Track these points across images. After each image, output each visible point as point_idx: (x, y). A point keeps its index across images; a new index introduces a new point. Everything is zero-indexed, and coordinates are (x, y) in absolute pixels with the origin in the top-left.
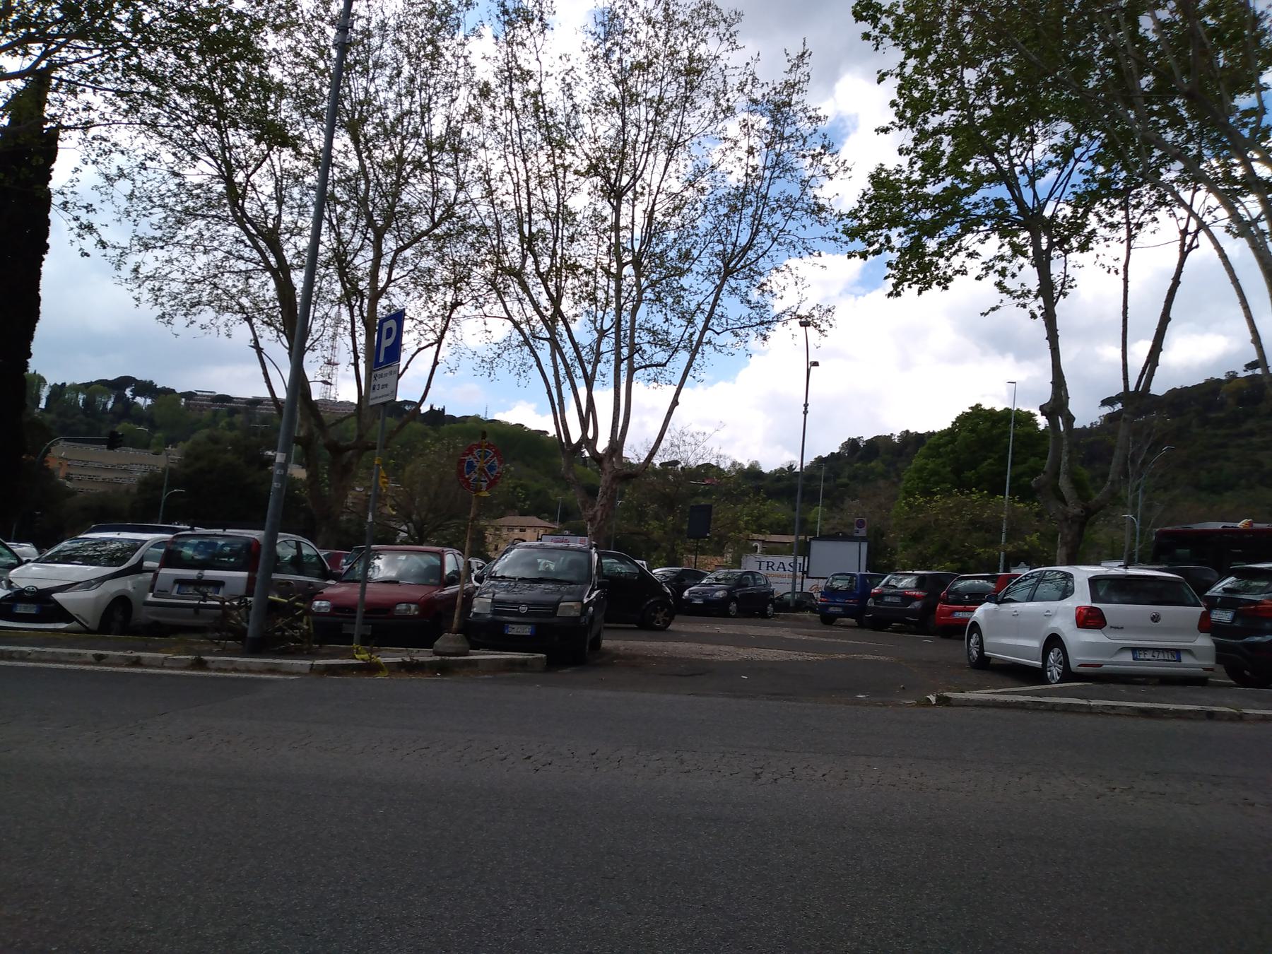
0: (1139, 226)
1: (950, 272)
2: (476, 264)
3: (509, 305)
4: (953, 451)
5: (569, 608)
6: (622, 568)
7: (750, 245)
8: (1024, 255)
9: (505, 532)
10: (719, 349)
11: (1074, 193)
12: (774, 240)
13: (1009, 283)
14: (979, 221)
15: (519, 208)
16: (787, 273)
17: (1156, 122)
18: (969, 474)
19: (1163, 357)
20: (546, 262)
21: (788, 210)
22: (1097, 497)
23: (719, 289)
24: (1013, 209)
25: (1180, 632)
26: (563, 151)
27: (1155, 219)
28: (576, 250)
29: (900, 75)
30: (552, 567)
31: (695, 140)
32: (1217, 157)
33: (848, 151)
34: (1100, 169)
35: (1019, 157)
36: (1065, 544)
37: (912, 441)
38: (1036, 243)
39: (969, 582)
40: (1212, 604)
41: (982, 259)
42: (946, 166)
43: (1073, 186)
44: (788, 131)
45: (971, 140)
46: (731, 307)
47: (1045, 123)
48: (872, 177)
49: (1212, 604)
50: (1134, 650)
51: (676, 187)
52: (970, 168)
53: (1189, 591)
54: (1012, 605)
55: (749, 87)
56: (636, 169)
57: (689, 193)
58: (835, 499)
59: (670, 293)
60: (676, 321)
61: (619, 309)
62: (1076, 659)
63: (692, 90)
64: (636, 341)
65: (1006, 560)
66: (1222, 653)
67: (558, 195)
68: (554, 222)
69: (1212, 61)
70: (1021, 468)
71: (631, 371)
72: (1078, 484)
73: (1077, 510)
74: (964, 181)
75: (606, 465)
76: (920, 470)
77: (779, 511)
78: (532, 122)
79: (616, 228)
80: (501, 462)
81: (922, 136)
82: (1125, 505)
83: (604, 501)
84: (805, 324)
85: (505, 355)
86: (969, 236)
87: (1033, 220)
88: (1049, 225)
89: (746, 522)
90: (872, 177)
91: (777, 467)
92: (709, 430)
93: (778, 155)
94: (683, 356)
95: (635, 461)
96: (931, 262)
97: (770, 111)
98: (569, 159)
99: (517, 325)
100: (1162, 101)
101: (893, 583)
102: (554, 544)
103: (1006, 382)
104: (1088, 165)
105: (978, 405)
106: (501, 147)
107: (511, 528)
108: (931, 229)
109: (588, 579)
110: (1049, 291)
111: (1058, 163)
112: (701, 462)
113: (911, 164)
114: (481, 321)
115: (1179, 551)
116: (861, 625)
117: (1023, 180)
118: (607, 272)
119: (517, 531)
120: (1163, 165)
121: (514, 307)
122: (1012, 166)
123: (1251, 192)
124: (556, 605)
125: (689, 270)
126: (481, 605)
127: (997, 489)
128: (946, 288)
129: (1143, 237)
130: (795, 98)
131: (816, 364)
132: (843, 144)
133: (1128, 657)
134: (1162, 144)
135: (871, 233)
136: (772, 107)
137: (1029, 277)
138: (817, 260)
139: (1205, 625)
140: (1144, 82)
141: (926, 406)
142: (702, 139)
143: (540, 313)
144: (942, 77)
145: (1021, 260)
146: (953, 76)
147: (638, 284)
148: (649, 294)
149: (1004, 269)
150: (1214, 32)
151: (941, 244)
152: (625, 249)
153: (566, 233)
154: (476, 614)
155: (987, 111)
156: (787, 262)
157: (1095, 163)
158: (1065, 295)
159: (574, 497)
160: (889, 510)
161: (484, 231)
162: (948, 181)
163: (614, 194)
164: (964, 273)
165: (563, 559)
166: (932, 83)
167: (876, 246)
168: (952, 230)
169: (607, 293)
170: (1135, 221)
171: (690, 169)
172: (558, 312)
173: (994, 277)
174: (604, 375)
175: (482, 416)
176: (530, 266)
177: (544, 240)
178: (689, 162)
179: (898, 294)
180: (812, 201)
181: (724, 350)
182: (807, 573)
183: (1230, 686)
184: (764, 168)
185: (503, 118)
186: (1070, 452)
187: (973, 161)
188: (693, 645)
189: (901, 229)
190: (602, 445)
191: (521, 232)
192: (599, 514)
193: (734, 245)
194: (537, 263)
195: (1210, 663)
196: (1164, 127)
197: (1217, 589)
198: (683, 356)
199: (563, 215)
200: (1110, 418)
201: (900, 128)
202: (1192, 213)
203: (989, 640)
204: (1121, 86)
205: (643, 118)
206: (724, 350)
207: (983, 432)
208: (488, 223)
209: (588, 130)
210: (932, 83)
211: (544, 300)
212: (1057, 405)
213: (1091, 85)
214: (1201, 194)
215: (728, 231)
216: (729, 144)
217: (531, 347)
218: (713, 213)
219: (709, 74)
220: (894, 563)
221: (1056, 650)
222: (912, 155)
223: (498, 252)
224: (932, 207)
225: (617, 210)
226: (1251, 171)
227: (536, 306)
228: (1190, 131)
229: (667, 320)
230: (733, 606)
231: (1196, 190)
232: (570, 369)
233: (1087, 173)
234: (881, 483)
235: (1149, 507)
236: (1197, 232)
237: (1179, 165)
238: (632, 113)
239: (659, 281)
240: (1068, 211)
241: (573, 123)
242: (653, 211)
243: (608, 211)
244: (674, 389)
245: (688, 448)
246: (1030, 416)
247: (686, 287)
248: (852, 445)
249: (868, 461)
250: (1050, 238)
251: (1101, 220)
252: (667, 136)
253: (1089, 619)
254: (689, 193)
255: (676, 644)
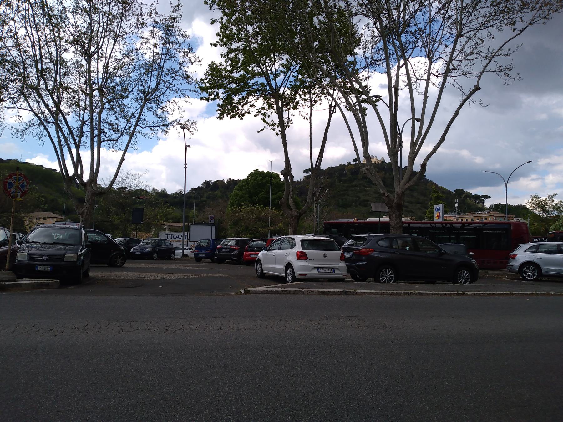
0: (315, 102)
1: (243, 112)
2: (11, 80)
3: (31, 104)
4: (248, 188)
5: (70, 257)
6: (99, 238)
7: (156, 89)
8: (273, 108)
9: (35, 220)
10: (144, 135)
11: (291, 85)
12: (168, 88)
13: (267, 119)
14: (255, 91)
15: (35, 55)
16: (175, 105)
17: (320, 61)
18: (255, 198)
19: (325, 155)
20: (51, 84)
21: (173, 75)
22: (303, 208)
23: (142, 107)
24: (268, 88)
25: (333, 261)
26: (59, 30)
27: (320, 100)
28: (67, 79)
29: (221, 22)
30: (61, 237)
31: (128, 35)
32: (341, 77)
33: (199, 52)
34: (300, 76)
35: (269, 67)
36: (292, 227)
37: (232, 183)
38: (277, 104)
39: (256, 242)
40: (345, 250)
41: (256, 108)
42: (241, 66)
43: (290, 82)
44: (172, 39)
45: (251, 56)
46: (148, 116)
47: (279, 54)
48: (210, 66)
49: (345, 250)
50: (318, 268)
51: (119, 56)
52: (250, 69)
53: (336, 245)
54: (273, 251)
55: (153, 15)
56: (98, 44)
57: (126, 60)
58: (201, 207)
59: (118, 106)
60: (121, 119)
61: (92, 112)
62: (297, 273)
63: (125, 11)
64: (102, 128)
65: (270, 234)
66: (349, 269)
67: (57, 51)
68: (55, 64)
69: (338, 41)
70: (274, 196)
71: (100, 142)
72: (296, 204)
73: (296, 214)
74: (248, 73)
75: (88, 188)
76: (236, 195)
77: (176, 212)
78: (41, 12)
79: (89, 71)
80: (28, 183)
81: (231, 51)
82: (313, 212)
83: (88, 205)
84: (183, 128)
85: (30, 129)
86: (251, 97)
87: (275, 94)
88: (282, 97)
89: (161, 216)
90: (210, 66)
91: (174, 192)
92: (140, 173)
93: (168, 49)
94: (126, 138)
95: (104, 186)
96: (236, 107)
97: (163, 28)
98: (62, 34)
99: (36, 114)
100: (322, 53)
101: (226, 243)
102: (61, 226)
103: (267, 161)
104: (296, 74)
105: (257, 170)
106: (23, 22)
107: (38, 218)
108: (236, 92)
109: (80, 243)
110: (283, 125)
111: (284, 72)
112: (137, 188)
113: (226, 62)
114: (16, 110)
115: (333, 230)
116: (213, 261)
117: (271, 77)
118: (85, 94)
119: (41, 219)
120: (323, 78)
121: (34, 105)
122: (267, 70)
123: (353, 93)
124: (63, 256)
125: (127, 97)
126: (22, 256)
127: (266, 205)
128: (242, 119)
129: (316, 106)
130: (175, 24)
131: (189, 146)
132: (197, 49)
133: (316, 271)
134: (322, 70)
135: (210, 91)
136: (164, 27)
137: (275, 118)
138: (187, 99)
139: (343, 258)
140: (315, 44)
141: (237, 169)
142: (131, 35)
143: (49, 109)
144: (238, 27)
145: (272, 110)
146: (243, 27)
147: (101, 100)
148: (107, 106)
149: (265, 113)
150: (338, 29)
151: (240, 99)
152: (94, 83)
153: (62, 71)
154: (19, 261)
155: (256, 45)
156: (174, 99)
157: (299, 74)
158: (289, 126)
159: (72, 203)
160: (224, 212)
161: (14, 64)
162: (242, 73)
163: (88, 55)
164: (249, 113)
165: (67, 233)
166: (235, 29)
167: (213, 96)
168: (244, 94)
169: (85, 103)
170: (313, 99)
171: (126, 49)
172: (59, 110)
173: (261, 116)
174: (86, 143)
175: (19, 160)
176: (42, 85)
177: (50, 73)
178: (125, 46)
179: (221, 119)
180: (184, 73)
181: (146, 136)
182: (189, 239)
183: (352, 281)
184: (162, 54)
185: (24, 7)
186: (292, 190)
187: (251, 66)
188: (136, 273)
189: (223, 90)
190: (86, 177)
191: (37, 67)
192: (86, 211)
193: (149, 87)
194: (46, 84)
195: (345, 273)
196: (323, 63)
197: (346, 245)
198: (126, 138)
199: (59, 62)
200: (307, 178)
201: (221, 46)
202: (333, 99)
203: (264, 266)
204: (307, 44)
205: (101, 21)
206: (146, 136)
207: (258, 179)
208: (17, 60)
209: (72, 21)
210: (235, 29)
211: (50, 103)
212: (287, 171)
213: (296, 41)
214: (336, 92)
215: (146, 81)
216: (144, 40)
217: (44, 126)
218: (138, 71)
219: (134, 5)
220: (227, 235)
221: (290, 269)
222: (227, 58)
223: (24, 77)
224: (235, 83)
225: (89, 63)
226: (352, 85)
227: (47, 106)
228: (332, 66)
229: (117, 119)
230: (155, 255)
231: (334, 90)
232: (67, 140)
233: (295, 77)
234: (220, 200)
235: (322, 213)
236: (335, 106)
237: (328, 79)
238: (96, 17)
239: (112, 100)
240: (288, 92)
241: (63, 16)
242: (107, 66)
243: (84, 62)
244: (122, 153)
245: (130, 181)
246: (278, 175)
247: (126, 104)
248: (207, 183)
249: (214, 191)
250: (282, 103)
251: (301, 97)
252: (114, 32)
253: (301, 256)
254: (126, 60)
255: (127, 273)
